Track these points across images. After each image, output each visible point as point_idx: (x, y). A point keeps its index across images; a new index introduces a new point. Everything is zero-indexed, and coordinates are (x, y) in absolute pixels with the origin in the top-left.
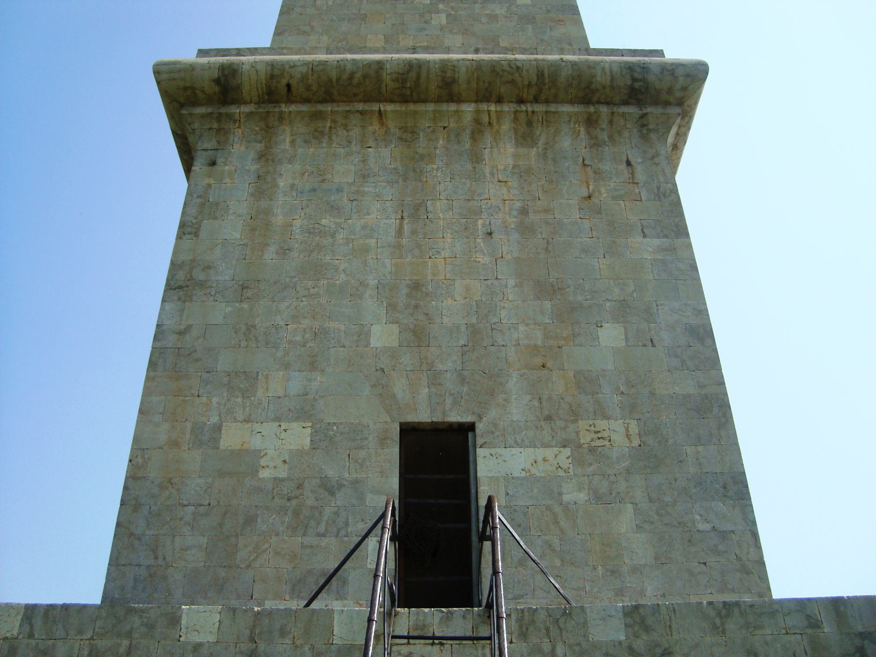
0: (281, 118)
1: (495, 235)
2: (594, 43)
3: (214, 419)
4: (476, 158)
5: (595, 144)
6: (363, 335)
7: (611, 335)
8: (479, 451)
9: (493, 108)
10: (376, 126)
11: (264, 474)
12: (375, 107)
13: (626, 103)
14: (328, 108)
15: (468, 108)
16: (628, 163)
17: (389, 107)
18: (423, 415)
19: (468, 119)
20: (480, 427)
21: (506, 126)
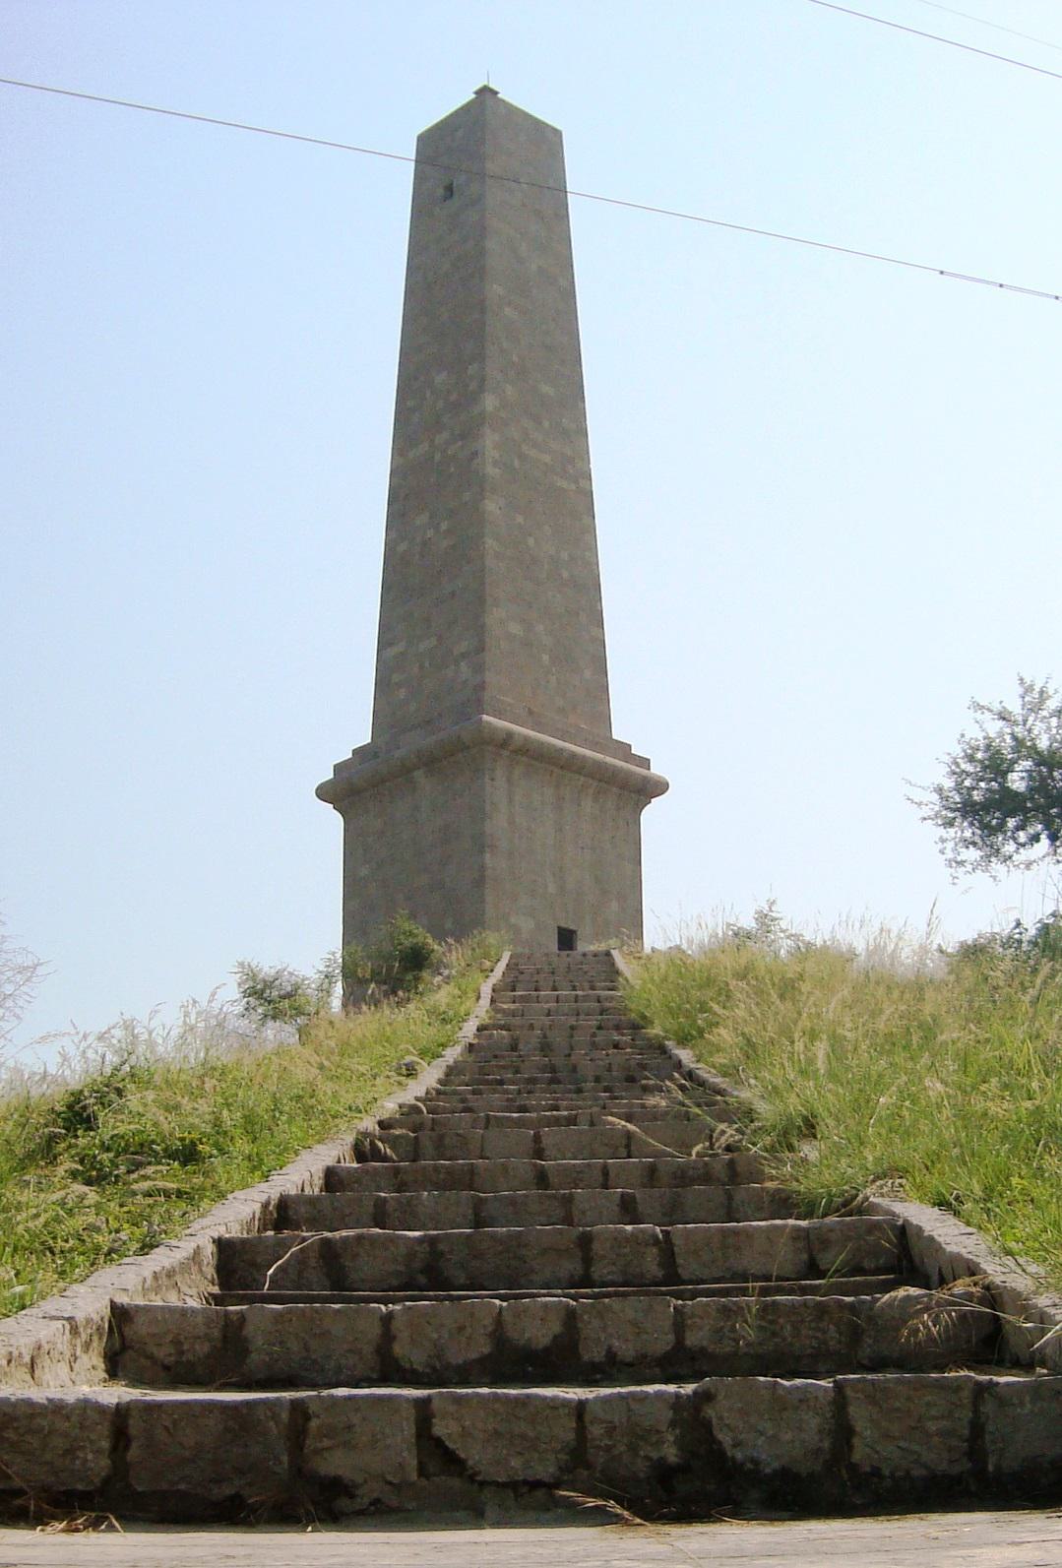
0: (517, 763)
1: (585, 850)
3: (507, 910)
4: (579, 805)
5: (618, 809)
6: (546, 887)
7: (614, 906)
8: (578, 943)
9: (591, 781)
10: (548, 777)
11: (523, 936)
12: (552, 768)
13: (634, 792)
14: (533, 762)
15: (582, 778)
16: (628, 823)
17: (556, 770)
18: (563, 925)
19: (581, 783)
20: (579, 933)
21: (591, 791)
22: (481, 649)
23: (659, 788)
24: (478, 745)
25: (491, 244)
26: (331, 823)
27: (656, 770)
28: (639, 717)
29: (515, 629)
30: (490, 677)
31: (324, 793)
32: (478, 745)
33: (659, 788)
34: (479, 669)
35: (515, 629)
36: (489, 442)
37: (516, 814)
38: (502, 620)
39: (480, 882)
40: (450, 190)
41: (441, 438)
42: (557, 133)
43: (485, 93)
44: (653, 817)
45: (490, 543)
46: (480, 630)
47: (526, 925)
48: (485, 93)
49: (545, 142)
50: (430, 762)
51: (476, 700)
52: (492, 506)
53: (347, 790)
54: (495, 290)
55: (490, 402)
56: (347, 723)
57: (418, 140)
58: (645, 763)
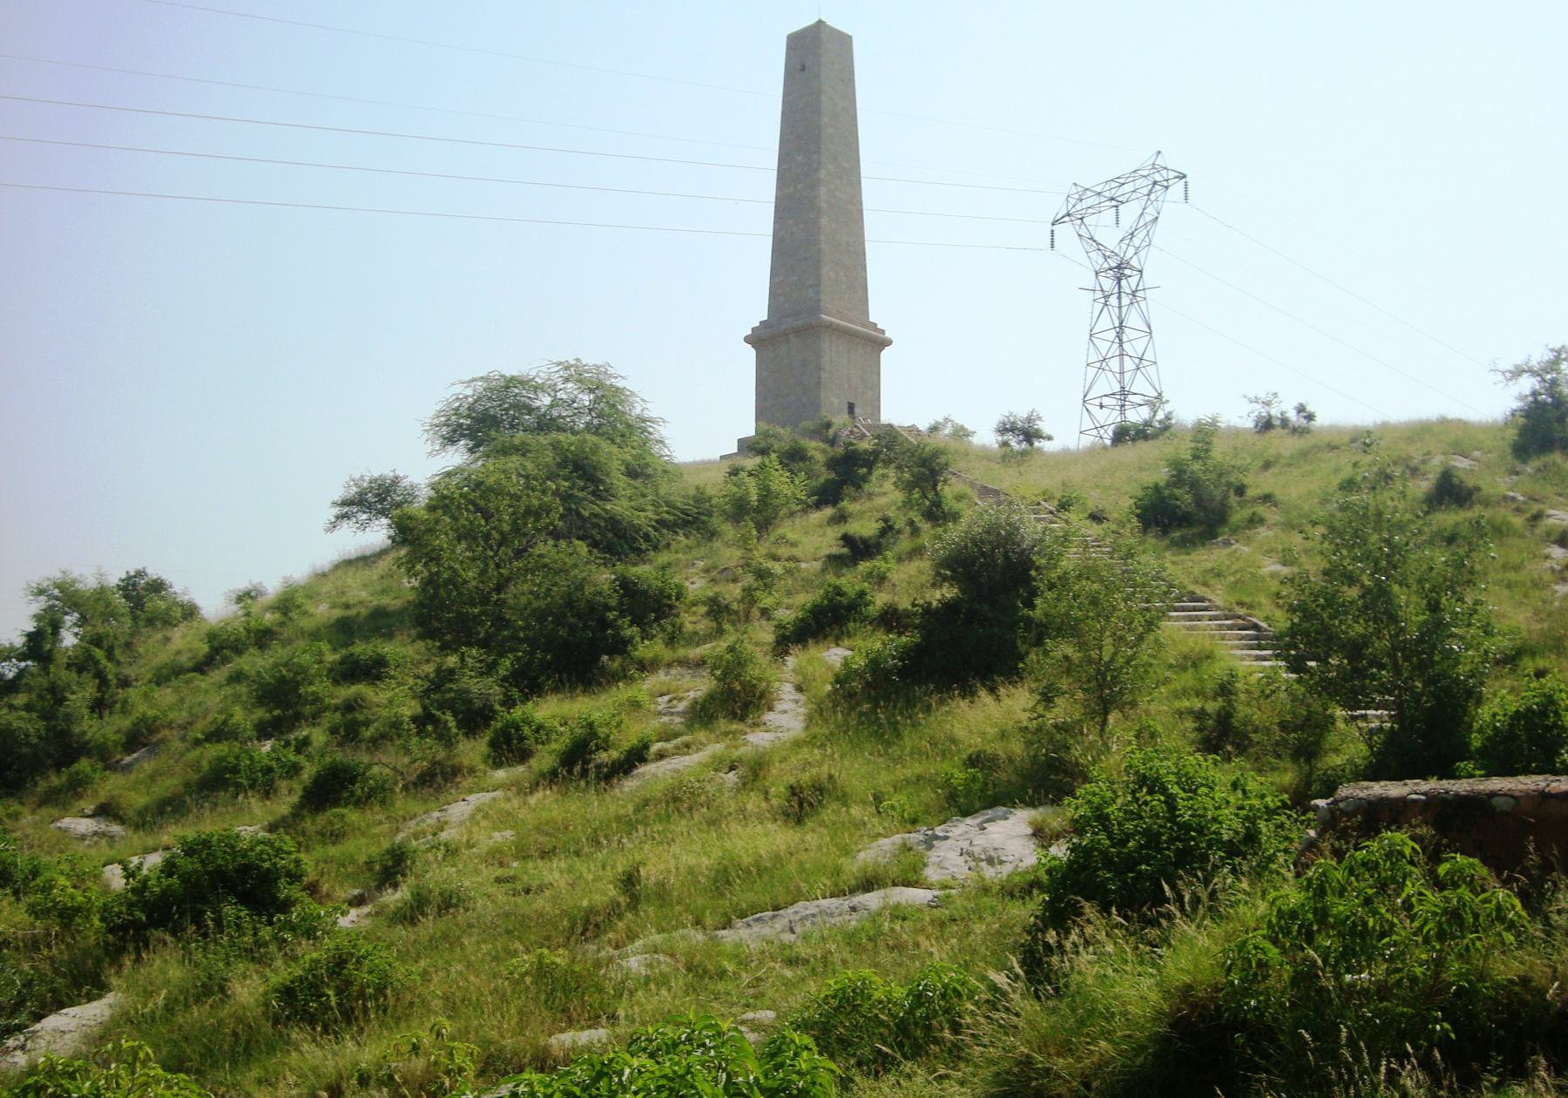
2: (872, 319)
22: (819, 285)
23: (888, 343)
24: (812, 323)
25: (824, 98)
26: (751, 353)
27: (887, 335)
28: (881, 311)
29: (832, 275)
30: (822, 297)
31: (747, 340)
32: (812, 323)
33: (888, 343)
34: (818, 293)
35: (832, 275)
36: (823, 191)
37: (834, 356)
38: (827, 271)
39: (819, 383)
40: (803, 68)
41: (800, 186)
42: (850, 37)
43: (820, 22)
44: (886, 355)
45: (822, 238)
46: (818, 276)
47: (836, 401)
48: (820, 22)
49: (845, 41)
50: (798, 332)
51: (816, 309)
52: (824, 221)
53: (758, 339)
54: (825, 120)
55: (823, 173)
56: (757, 310)
57: (789, 47)
58: (883, 332)
